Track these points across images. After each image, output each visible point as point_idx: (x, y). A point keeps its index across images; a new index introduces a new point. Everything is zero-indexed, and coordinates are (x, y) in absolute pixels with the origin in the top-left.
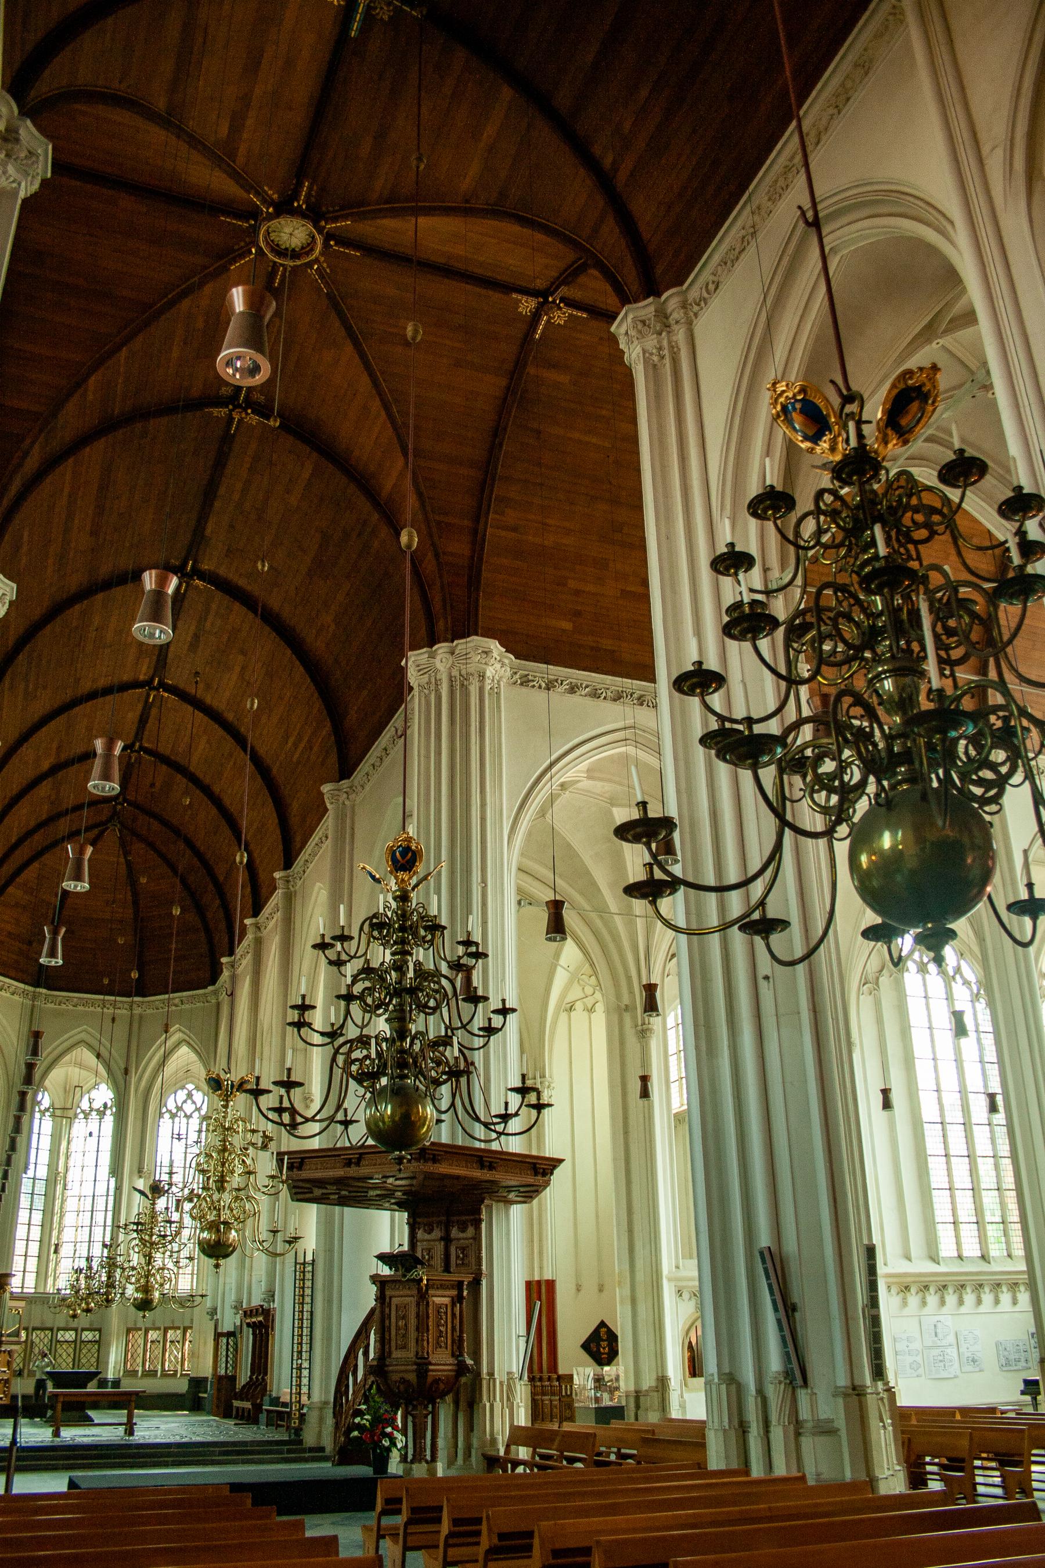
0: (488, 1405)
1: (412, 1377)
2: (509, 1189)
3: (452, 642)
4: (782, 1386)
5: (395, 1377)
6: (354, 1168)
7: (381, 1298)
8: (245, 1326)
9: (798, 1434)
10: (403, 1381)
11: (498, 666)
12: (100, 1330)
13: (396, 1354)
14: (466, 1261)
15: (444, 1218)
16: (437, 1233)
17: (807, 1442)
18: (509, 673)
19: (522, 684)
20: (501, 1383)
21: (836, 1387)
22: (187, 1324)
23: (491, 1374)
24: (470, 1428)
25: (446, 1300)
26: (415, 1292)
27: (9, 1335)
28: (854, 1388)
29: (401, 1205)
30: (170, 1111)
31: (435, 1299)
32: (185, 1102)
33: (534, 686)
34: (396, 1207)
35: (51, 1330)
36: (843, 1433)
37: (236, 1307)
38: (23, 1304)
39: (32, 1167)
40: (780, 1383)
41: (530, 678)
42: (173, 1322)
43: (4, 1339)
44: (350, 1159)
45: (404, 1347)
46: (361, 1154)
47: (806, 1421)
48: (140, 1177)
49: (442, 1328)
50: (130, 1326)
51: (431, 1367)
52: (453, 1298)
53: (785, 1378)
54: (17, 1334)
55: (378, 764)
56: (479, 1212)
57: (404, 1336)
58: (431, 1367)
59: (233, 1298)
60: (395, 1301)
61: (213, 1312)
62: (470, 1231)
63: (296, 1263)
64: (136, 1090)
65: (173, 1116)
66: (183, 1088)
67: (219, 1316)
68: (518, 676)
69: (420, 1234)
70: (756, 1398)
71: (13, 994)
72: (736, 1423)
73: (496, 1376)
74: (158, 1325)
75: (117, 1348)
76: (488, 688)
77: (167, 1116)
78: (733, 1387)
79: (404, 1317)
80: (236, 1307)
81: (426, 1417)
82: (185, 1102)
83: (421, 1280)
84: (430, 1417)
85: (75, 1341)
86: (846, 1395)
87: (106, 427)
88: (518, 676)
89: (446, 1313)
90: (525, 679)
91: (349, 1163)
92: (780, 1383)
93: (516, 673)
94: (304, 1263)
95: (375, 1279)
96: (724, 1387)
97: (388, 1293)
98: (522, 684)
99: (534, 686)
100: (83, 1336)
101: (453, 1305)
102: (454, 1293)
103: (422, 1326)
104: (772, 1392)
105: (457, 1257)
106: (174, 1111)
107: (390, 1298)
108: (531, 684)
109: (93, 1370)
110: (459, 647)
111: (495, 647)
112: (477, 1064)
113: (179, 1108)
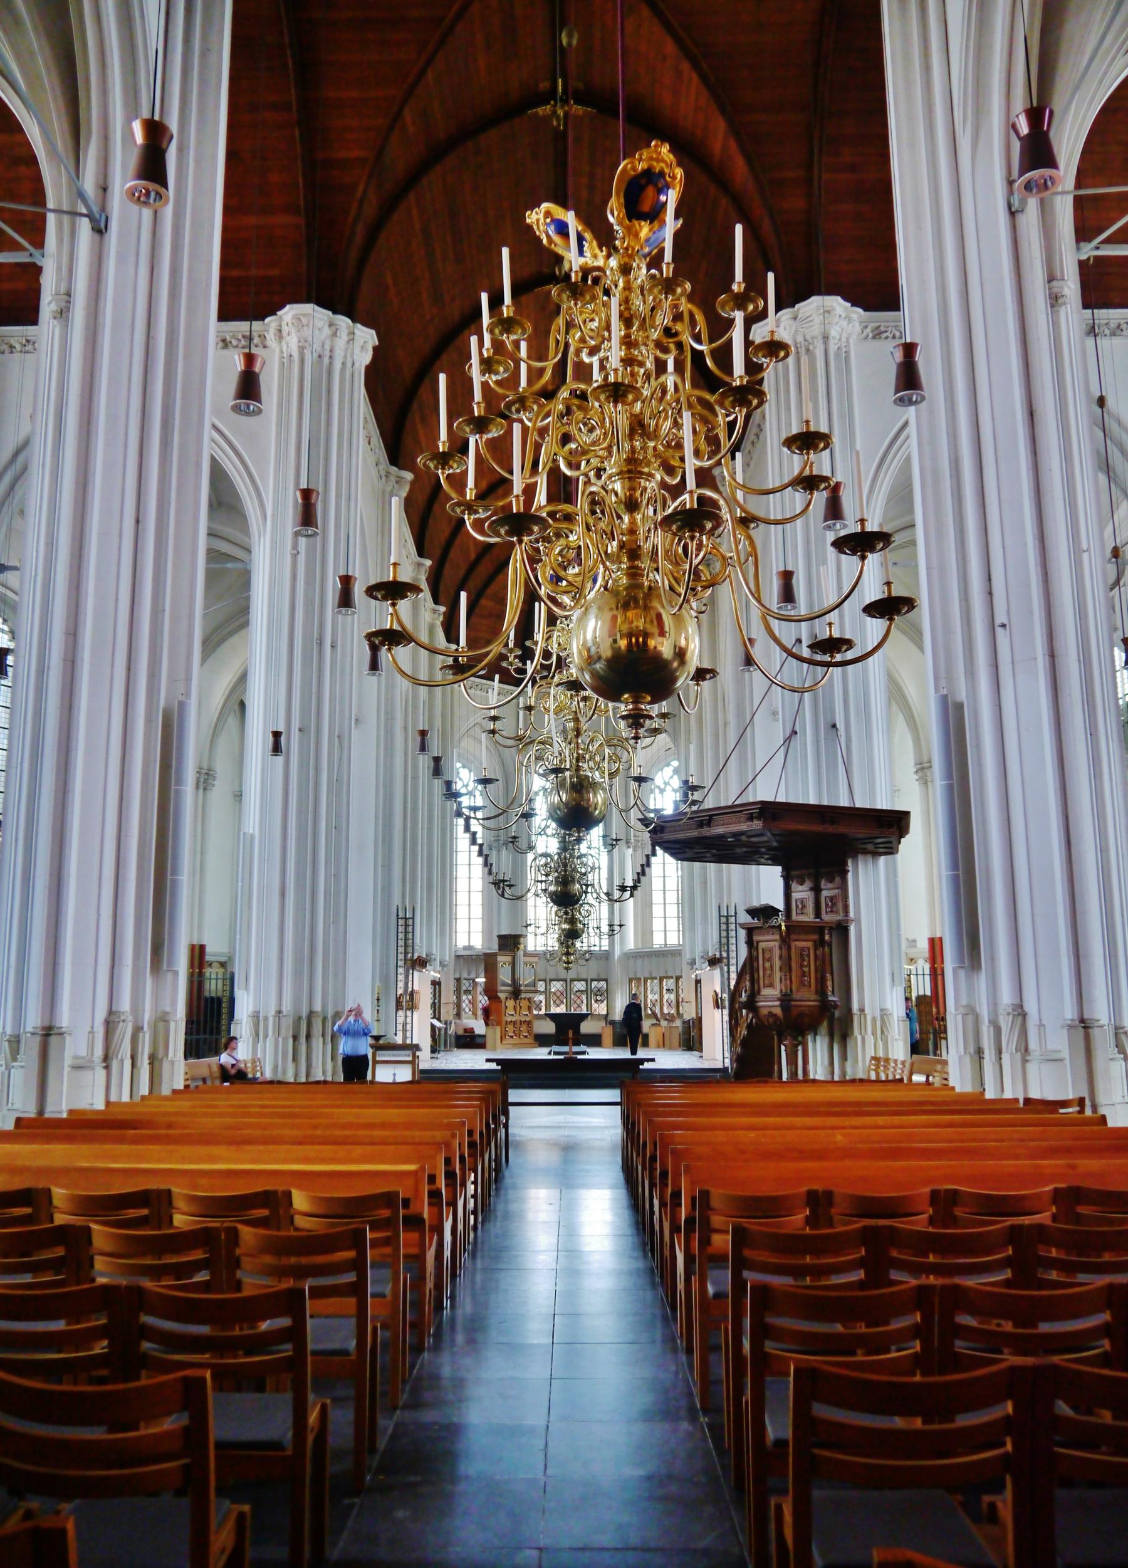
0: (859, 1038)
1: (778, 1011)
2: (865, 841)
3: (794, 306)
4: (1011, 1017)
5: (764, 1012)
6: (706, 829)
7: (750, 942)
9: (1025, 1061)
10: (771, 1014)
11: (844, 323)
12: (606, 980)
13: (766, 992)
14: (835, 909)
15: (812, 871)
16: (808, 884)
17: (1032, 1068)
18: (857, 328)
19: (874, 337)
20: (874, 1019)
21: (1065, 1020)
22: (678, 974)
23: (862, 1010)
24: (844, 1057)
25: (810, 944)
26: (777, 937)
27: (526, 986)
28: (1082, 1021)
29: (775, 861)
31: (797, 943)
32: (672, 777)
33: (887, 338)
34: (770, 862)
35: (565, 980)
36: (1067, 1062)
37: (703, 957)
38: (535, 959)
40: (1008, 1014)
41: (882, 329)
42: (666, 972)
43: (522, 988)
44: (702, 821)
45: (771, 985)
46: (711, 816)
47: (1035, 1051)
48: (629, 847)
49: (806, 969)
50: (632, 976)
51: (793, 1003)
52: (814, 941)
53: (1013, 1010)
55: (756, 441)
56: (846, 864)
57: (770, 976)
58: (793, 1003)
59: (700, 950)
60: (762, 945)
62: (838, 880)
63: (720, 916)
65: (662, 791)
66: (668, 765)
68: (869, 330)
69: (794, 886)
70: (989, 1027)
72: (972, 1050)
73: (867, 1011)
74: (654, 975)
76: (832, 348)
77: (657, 791)
78: (970, 1018)
79: (770, 960)
81: (797, 1046)
82: (672, 777)
83: (780, 926)
84: (800, 1048)
85: (586, 991)
86: (1070, 1027)
87: (436, 154)
88: (869, 330)
89: (809, 955)
90: (876, 332)
91: (701, 825)
92: (1008, 1014)
93: (866, 327)
94: (727, 917)
95: (742, 926)
96: (960, 1017)
97: (756, 938)
98: (874, 337)
99: (887, 338)
100: (593, 986)
101: (815, 950)
102: (815, 937)
103: (787, 967)
104: (1005, 1023)
105: (827, 905)
106: (662, 786)
107: (758, 942)
108: (884, 335)
109: (584, 1011)
110: (801, 311)
111: (837, 304)
112: (838, 726)
113: (666, 784)
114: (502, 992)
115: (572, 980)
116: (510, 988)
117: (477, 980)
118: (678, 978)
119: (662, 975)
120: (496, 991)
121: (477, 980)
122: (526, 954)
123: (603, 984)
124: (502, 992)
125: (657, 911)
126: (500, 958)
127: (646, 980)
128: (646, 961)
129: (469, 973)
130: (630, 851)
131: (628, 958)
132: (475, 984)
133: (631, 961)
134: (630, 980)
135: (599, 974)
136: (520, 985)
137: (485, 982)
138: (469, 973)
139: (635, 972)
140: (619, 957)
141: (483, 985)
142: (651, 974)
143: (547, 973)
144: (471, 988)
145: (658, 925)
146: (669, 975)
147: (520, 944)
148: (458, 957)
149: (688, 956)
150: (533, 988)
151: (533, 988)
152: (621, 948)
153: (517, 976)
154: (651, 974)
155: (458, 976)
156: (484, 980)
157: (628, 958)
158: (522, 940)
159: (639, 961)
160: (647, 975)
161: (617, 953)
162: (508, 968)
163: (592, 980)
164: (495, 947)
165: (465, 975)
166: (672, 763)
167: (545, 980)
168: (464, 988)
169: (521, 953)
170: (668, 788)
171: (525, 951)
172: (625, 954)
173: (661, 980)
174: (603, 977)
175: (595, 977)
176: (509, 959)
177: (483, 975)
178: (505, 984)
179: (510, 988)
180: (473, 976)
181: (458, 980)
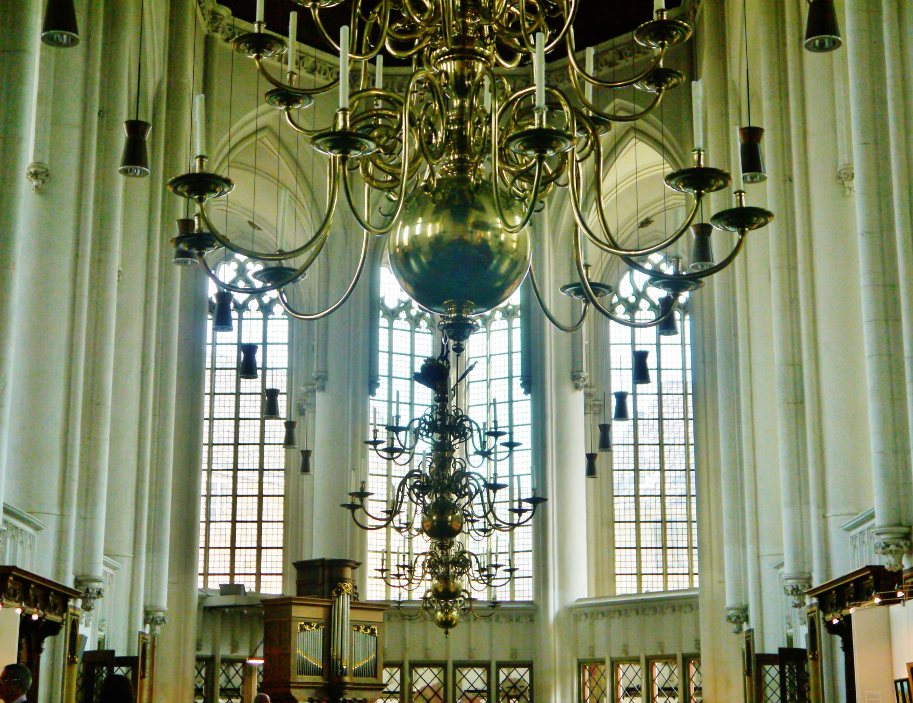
8: (823, 631)
12: (529, 665)
22: (689, 649)
27: (356, 674)
30: (625, 301)
35: (442, 665)
37: (796, 591)
38: (378, 617)
39: (383, 382)
42: (661, 645)
43: (347, 679)
48: (577, 387)
50: (584, 655)
54: (373, 670)
61: (741, 616)
64: (554, 233)
67: (753, 623)
71: (312, 71)
74: (633, 653)
75: (563, 696)
80: (796, 591)
100: (502, 677)
106: (632, 300)
113: (640, 295)
114: (301, 686)
115: (458, 665)
116: (318, 679)
117: (251, 661)
118: (689, 659)
119: (652, 651)
120: (287, 685)
121: (251, 661)
122: (358, 605)
123: (520, 674)
124: (301, 686)
125: (624, 535)
126: (300, 612)
127: (615, 664)
128: (617, 623)
129: (235, 647)
130: (580, 394)
131: (577, 618)
132: (248, 670)
133: (584, 624)
134: (581, 665)
135: (514, 653)
136: (344, 673)
137: (264, 665)
138: (235, 647)
139: (592, 648)
140: (558, 618)
141: (261, 669)
142: (626, 651)
143: (404, 649)
144: (237, 682)
145: (624, 561)
146: (669, 651)
147: (343, 580)
148: (209, 611)
149: (729, 602)
150: (371, 680)
151: (371, 680)
152: (562, 597)
153: (335, 653)
154: (626, 651)
155: (206, 652)
156: (262, 662)
157: (577, 618)
158: (348, 573)
159: (600, 625)
160: (617, 653)
161: (554, 606)
162: (316, 635)
163: (500, 665)
164: (292, 592)
165: (225, 651)
166: (651, 257)
167: (400, 665)
168: (221, 681)
169: (345, 601)
170: (644, 304)
171: (355, 597)
172: (570, 609)
173: (649, 663)
174: (522, 657)
175: (506, 658)
176: (318, 613)
177: (260, 652)
178: (306, 669)
179: (318, 679)
180: (243, 652)
181: (207, 663)
